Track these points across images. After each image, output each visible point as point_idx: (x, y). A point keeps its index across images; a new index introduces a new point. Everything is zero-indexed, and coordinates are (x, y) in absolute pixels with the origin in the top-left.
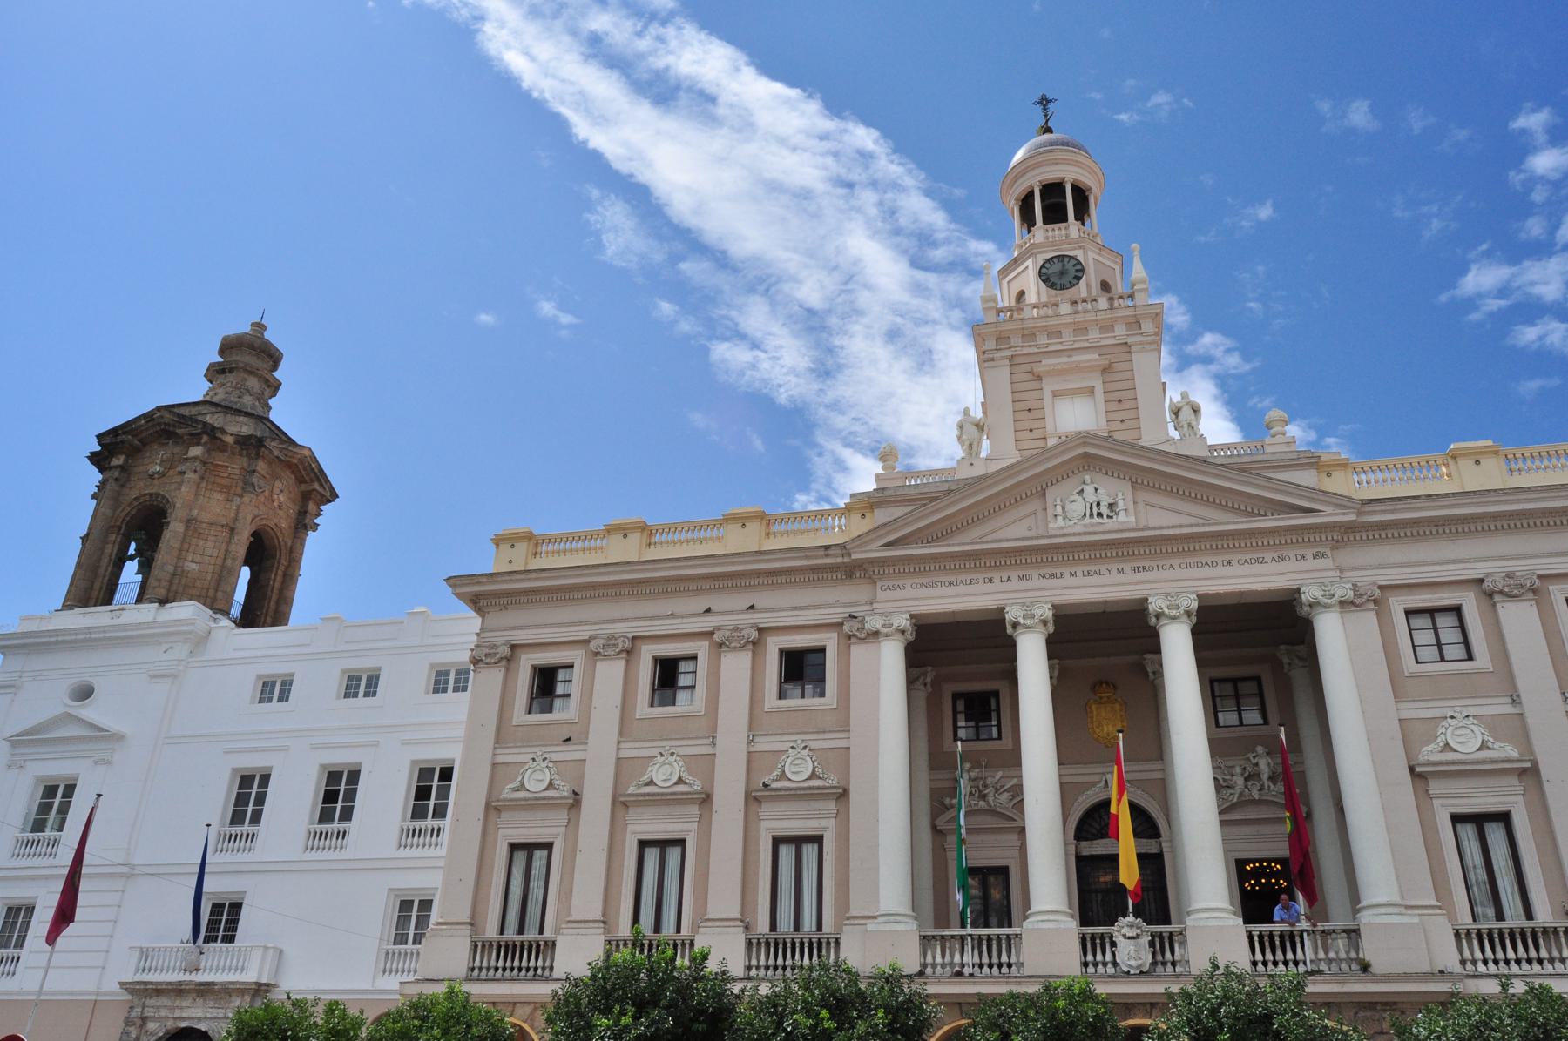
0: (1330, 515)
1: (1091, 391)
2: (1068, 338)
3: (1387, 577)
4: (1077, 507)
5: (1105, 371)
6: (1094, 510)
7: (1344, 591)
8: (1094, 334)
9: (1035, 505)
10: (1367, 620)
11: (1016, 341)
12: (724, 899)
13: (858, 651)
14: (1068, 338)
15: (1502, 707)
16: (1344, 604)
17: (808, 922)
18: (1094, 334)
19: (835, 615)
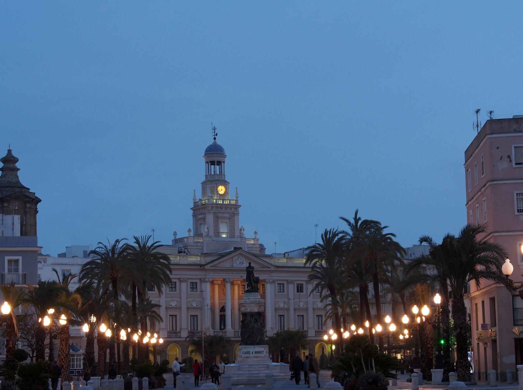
0: (272, 269)
1: (227, 223)
2: (224, 209)
3: (277, 278)
4: (238, 263)
5: (230, 219)
6: (240, 263)
7: (271, 281)
8: (228, 210)
9: (231, 260)
10: (273, 285)
11: (214, 208)
12: (184, 326)
13: (203, 284)
14: (224, 209)
15: (286, 300)
16: (271, 283)
17: (199, 329)
18: (228, 210)
19: (199, 277)
